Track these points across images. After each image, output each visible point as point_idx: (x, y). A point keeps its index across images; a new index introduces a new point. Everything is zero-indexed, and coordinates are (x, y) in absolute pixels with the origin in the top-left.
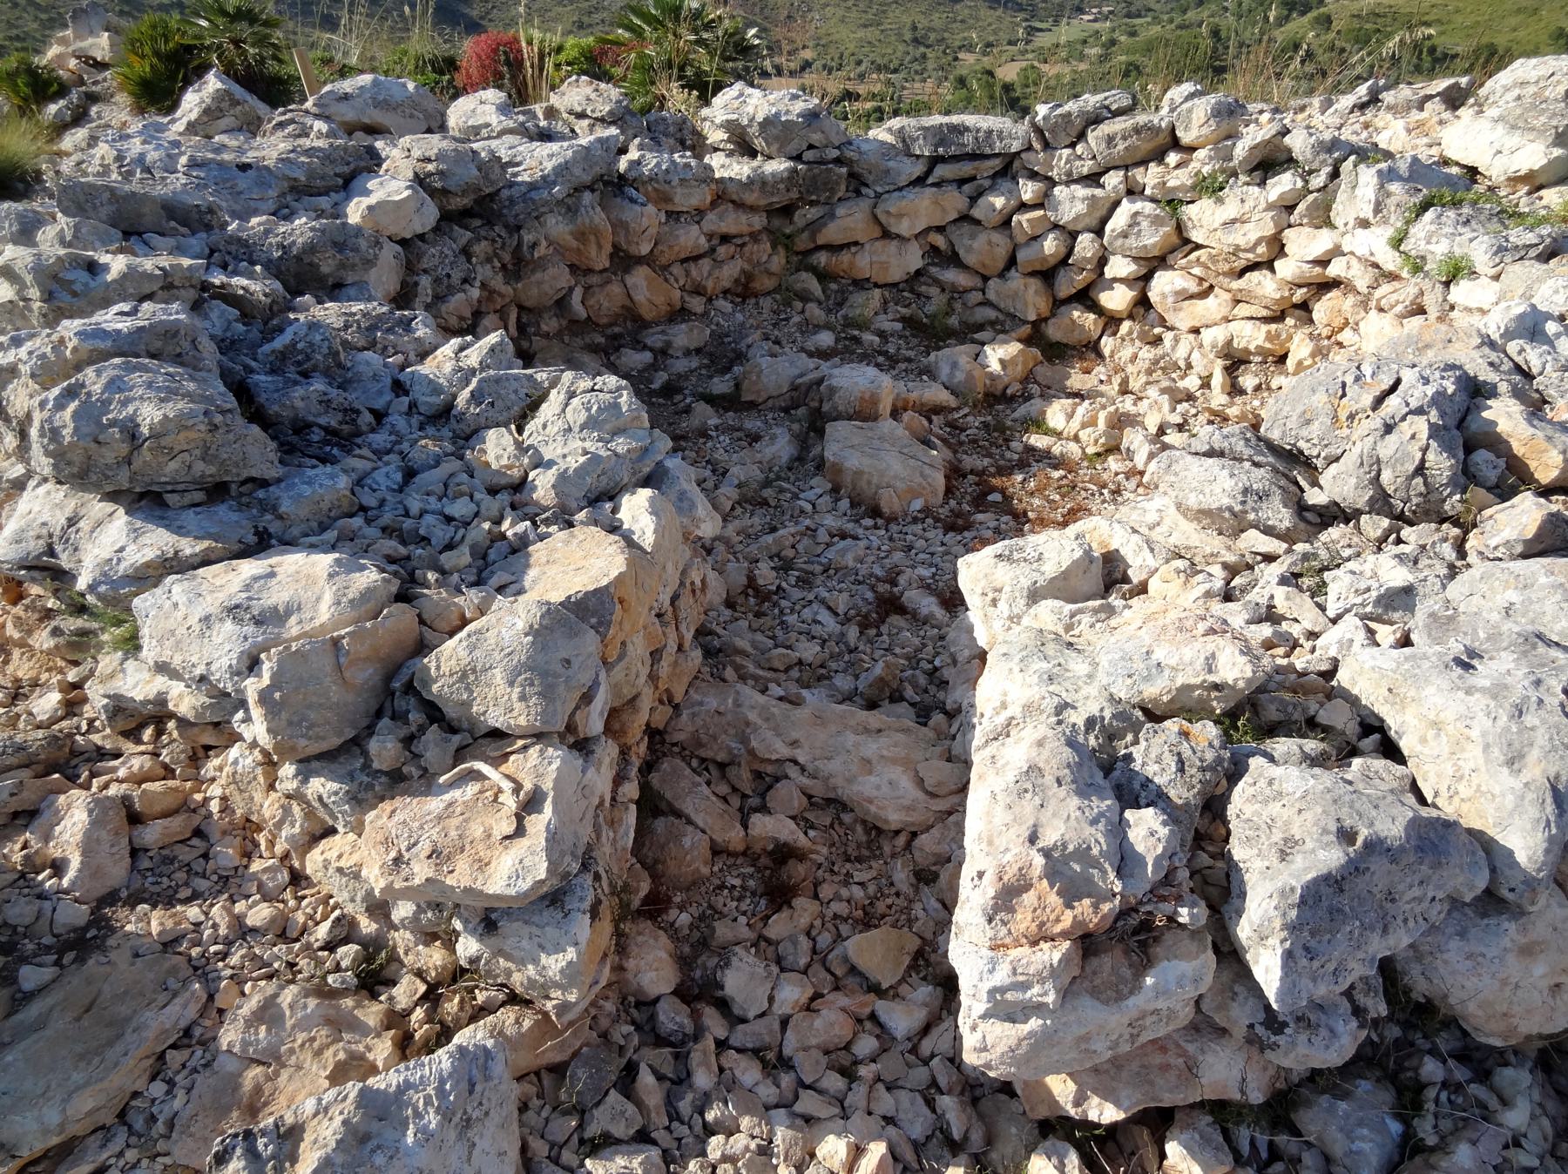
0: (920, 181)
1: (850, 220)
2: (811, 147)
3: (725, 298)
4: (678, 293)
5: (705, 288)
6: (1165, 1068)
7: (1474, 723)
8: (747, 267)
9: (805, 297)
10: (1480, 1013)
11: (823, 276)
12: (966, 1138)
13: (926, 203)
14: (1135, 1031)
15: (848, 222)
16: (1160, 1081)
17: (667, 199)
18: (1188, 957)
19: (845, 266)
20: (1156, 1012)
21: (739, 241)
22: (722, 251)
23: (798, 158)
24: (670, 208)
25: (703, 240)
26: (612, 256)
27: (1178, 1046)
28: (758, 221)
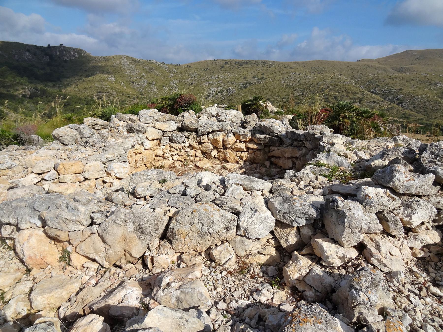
0: (291, 145)
1: (277, 151)
2: (271, 132)
3: (249, 162)
8: (255, 156)
9: (265, 167)
11: (272, 163)
13: (290, 150)
15: (277, 151)
19: (277, 162)
23: (269, 135)
28: (260, 147)
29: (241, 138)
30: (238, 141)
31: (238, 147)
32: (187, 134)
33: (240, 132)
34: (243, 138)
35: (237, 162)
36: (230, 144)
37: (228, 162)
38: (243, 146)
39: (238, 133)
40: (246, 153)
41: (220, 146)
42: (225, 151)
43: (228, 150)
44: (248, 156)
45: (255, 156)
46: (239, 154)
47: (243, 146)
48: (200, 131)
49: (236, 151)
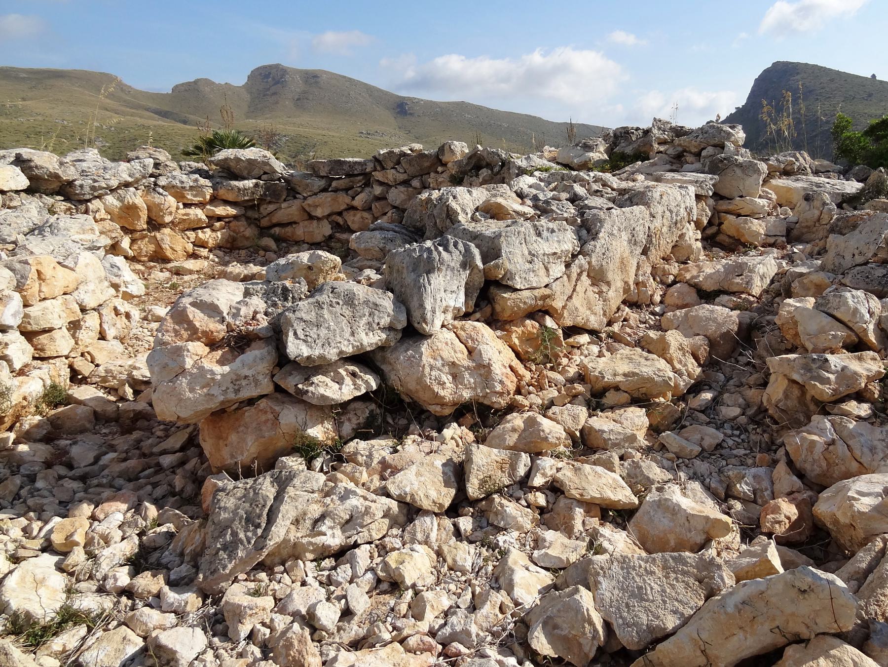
4: (191, 245)
5: (207, 242)
6: (266, 421)
7: (405, 261)
8: (232, 233)
10: (418, 387)
12: (182, 490)
14: (236, 387)
16: (264, 428)
17: (184, 197)
18: (259, 349)
20: (246, 377)
21: (227, 220)
22: (218, 224)
24: (186, 202)
25: (204, 217)
26: (148, 223)
27: (271, 408)
29: (189, 197)
30: (181, 206)
31: (192, 217)
32: (49, 200)
33: (182, 182)
34: (195, 196)
35: (194, 256)
36: (171, 213)
37: (169, 261)
38: (199, 214)
39: (179, 185)
40: (207, 230)
41: (142, 224)
42: (158, 235)
43: (167, 231)
44: (219, 234)
45: (232, 233)
46: (192, 235)
47: (199, 214)
48: (87, 189)
49: (183, 231)
